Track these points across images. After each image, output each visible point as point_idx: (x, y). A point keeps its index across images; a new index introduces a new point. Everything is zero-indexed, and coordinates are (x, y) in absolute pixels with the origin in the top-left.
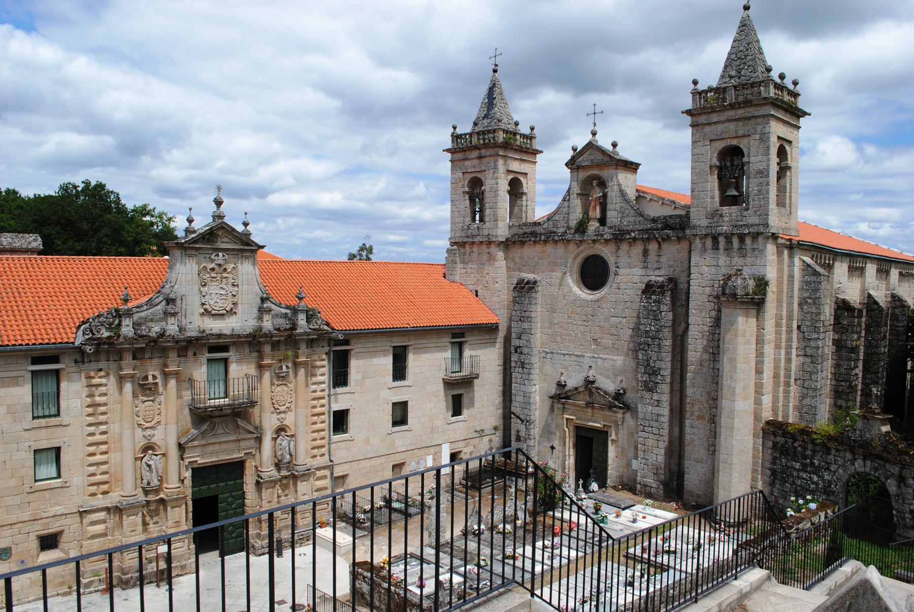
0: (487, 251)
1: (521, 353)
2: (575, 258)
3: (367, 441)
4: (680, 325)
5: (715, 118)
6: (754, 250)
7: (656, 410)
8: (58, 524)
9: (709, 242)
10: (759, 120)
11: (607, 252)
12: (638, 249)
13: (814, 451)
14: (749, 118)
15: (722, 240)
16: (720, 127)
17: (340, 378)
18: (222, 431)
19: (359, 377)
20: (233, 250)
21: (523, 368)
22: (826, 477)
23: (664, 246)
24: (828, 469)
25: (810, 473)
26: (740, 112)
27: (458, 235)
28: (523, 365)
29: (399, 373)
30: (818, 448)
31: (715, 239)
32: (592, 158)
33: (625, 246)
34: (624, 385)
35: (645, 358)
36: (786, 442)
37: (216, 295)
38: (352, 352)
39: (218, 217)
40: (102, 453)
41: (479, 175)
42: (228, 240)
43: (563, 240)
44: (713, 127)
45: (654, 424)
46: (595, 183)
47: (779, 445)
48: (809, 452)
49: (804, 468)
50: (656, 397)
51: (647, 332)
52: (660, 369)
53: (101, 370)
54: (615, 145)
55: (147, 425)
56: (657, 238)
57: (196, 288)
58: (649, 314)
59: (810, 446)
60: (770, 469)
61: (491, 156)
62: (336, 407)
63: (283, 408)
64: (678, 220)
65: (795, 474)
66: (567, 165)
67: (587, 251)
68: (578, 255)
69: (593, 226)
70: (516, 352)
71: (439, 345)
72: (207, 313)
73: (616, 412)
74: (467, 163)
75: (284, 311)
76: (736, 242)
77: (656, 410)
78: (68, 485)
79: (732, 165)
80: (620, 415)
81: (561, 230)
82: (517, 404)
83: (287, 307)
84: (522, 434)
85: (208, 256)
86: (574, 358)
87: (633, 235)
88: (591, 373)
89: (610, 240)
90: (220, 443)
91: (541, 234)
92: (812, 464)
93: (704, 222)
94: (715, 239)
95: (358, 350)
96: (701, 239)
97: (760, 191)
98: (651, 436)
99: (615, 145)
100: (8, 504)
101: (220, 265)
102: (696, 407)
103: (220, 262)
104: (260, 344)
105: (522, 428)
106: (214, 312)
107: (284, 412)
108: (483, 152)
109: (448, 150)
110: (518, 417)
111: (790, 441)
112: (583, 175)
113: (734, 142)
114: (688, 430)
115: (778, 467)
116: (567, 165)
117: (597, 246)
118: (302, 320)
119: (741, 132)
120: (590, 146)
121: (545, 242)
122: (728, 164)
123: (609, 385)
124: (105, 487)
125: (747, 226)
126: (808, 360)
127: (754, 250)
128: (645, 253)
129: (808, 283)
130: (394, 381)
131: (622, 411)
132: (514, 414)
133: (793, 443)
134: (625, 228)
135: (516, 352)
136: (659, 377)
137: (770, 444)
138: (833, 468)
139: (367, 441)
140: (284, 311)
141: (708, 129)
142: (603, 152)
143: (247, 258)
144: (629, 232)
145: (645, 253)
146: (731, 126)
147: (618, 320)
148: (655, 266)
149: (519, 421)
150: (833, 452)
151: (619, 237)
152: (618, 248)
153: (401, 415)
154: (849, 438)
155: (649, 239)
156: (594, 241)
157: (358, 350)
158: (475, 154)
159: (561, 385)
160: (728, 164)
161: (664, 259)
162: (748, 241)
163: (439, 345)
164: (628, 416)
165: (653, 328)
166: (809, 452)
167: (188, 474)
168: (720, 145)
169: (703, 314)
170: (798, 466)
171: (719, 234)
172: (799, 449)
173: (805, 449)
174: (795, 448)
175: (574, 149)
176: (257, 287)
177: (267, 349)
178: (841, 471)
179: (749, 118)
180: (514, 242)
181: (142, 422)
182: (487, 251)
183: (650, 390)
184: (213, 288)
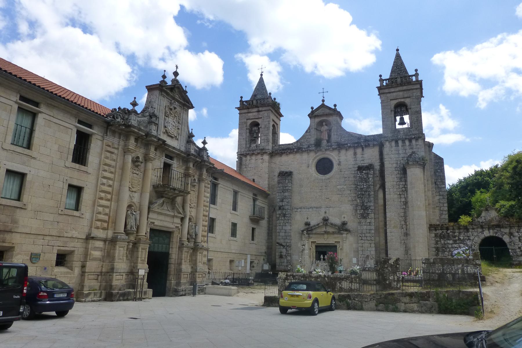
0: (261, 158)
1: (284, 209)
2: (314, 160)
4: (376, 186)
5: (392, 90)
6: (417, 145)
7: (369, 227)
8: (72, 245)
9: (393, 143)
10: (414, 91)
11: (333, 156)
12: (351, 152)
13: (460, 233)
14: (409, 90)
15: (400, 143)
16: (395, 94)
21: (284, 217)
22: (468, 244)
23: (366, 150)
24: (469, 239)
25: (459, 244)
26: (405, 88)
27: (243, 150)
28: (284, 215)
30: (462, 231)
31: (397, 142)
32: (323, 111)
33: (343, 152)
34: (346, 219)
35: (361, 202)
36: (443, 232)
38: (219, 186)
40: (108, 200)
41: (257, 120)
43: (308, 150)
44: (391, 94)
45: (368, 235)
46: (324, 124)
47: (438, 235)
48: (457, 234)
49: (455, 242)
50: (368, 221)
51: (361, 189)
52: (370, 206)
54: (335, 106)
56: (362, 146)
58: (362, 180)
59: (457, 231)
60: (435, 248)
61: (265, 110)
64: (372, 138)
65: (450, 246)
66: (309, 115)
67: (320, 155)
68: (315, 158)
69: (324, 143)
70: (280, 209)
73: (342, 234)
74: (249, 114)
75: (196, 149)
76: (407, 143)
77: (369, 227)
79: (401, 111)
80: (344, 235)
81: (305, 147)
82: (280, 237)
84: (284, 254)
86: (315, 209)
87: (349, 145)
88: (327, 215)
89: (336, 149)
91: (294, 149)
92: (459, 239)
93: (390, 135)
94: (397, 142)
96: (389, 142)
97: (417, 120)
98: (366, 242)
99: (335, 106)
100: (45, 219)
102: (392, 222)
105: (284, 250)
108: (260, 109)
109: (238, 108)
110: (281, 245)
111: (445, 231)
112: (317, 120)
113: (402, 100)
114: (388, 234)
115: (439, 245)
116: (309, 115)
117: (328, 152)
119: (406, 96)
120: (323, 106)
121: (296, 152)
122: (399, 110)
123: (336, 221)
125: (413, 134)
126: (441, 197)
127: (417, 145)
128: (355, 154)
129: (437, 163)
131: (346, 233)
132: (278, 243)
133: (447, 232)
134: (343, 143)
135: (280, 209)
136: (370, 210)
137: (433, 235)
138: (472, 238)
141: (389, 95)
142: (330, 109)
144: (347, 144)
145: (355, 154)
146: (401, 93)
147: (341, 187)
148: (361, 159)
149: (282, 247)
150: (470, 230)
151: (340, 147)
152: (340, 152)
154: (479, 222)
155: (357, 147)
156: (326, 150)
158: (255, 110)
159: (307, 224)
160: (399, 110)
161: (365, 156)
162: (414, 142)
164: (349, 235)
165: (365, 186)
166: (457, 234)
167: (149, 230)
168: (394, 102)
169: (393, 176)
170: (451, 242)
171: (399, 139)
172: (451, 233)
173: (454, 233)
174: (448, 233)
175: (312, 108)
178: (476, 238)
179: (409, 90)
180: (276, 154)
182: (261, 158)
183: (365, 218)
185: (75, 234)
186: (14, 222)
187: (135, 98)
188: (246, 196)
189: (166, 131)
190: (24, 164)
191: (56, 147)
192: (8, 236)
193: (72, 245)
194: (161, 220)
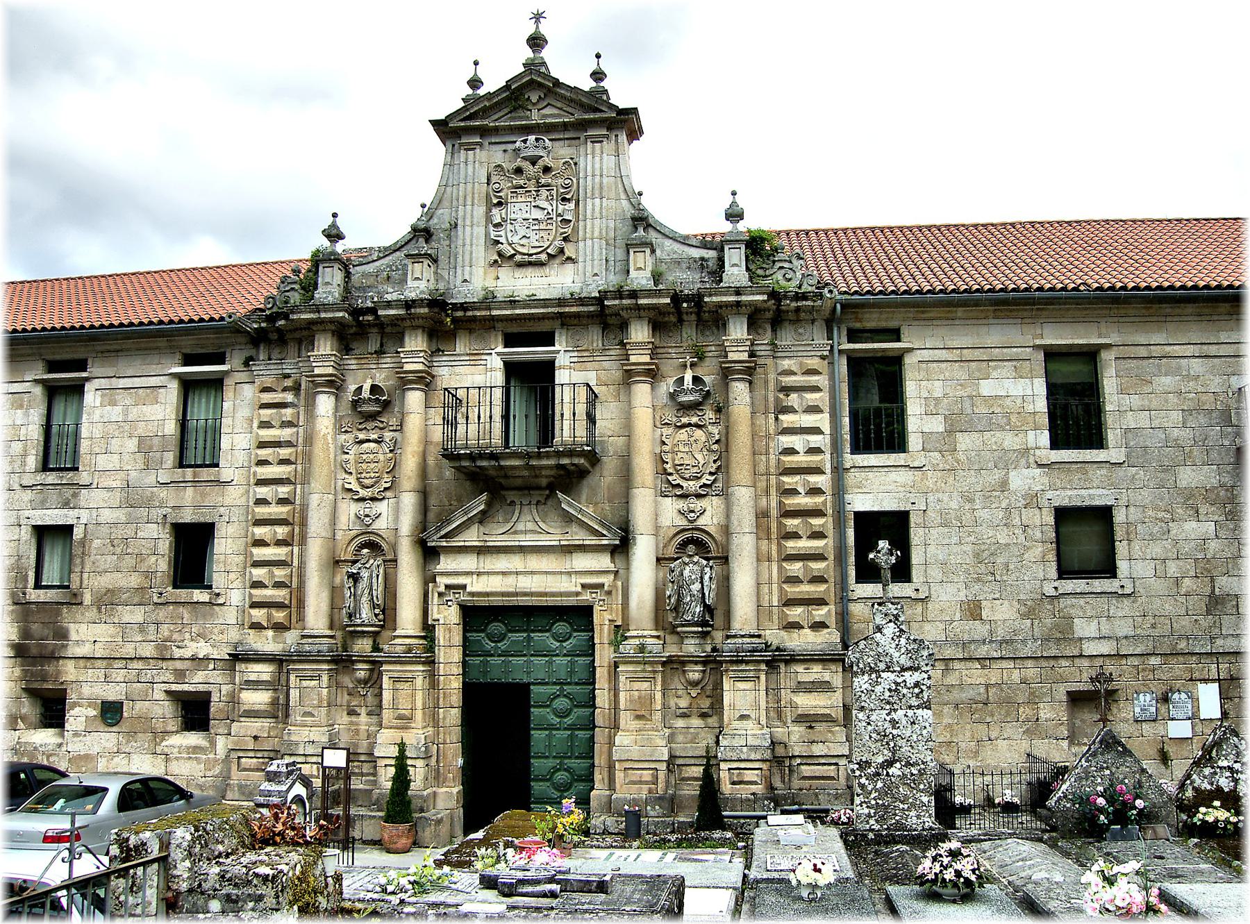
3: (973, 611)
17: (877, 423)
18: (530, 526)
19: (936, 425)
20: (565, 127)
29: (1076, 417)
37: (526, 221)
38: (909, 360)
39: (532, 67)
40: (279, 543)
42: (556, 111)
53: (287, 376)
55: (363, 493)
57: (480, 210)
62: (860, 502)
63: (692, 486)
71: (1213, 350)
72: (503, 259)
75: (697, 253)
78: (221, 601)
83: (705, 245)
85: (510, 147)
90: (522, 550)
95: (926, 355)
100: (125, 620)
101: (534, 161)
103: (530, 153)
104: (624, 326)
106: (518, 258)
107: (699, 496)
118: (736, 271)
124: (279, 616)
130: (1055, 445)
139: (973, 611)
140: (697, 253)
143: (597, 140)
153: (1085, 539)
157: (926, 355)
163: (1213, 350)
176: (625, 203)
177: (640, 333)
181: (354, 486)
184: (520, 209)
185: (202, 649)
186: (63, 635)
187: (335, 215)
188: (1189, 350)
189: (500, 254)
190: (66, 505)
191: (132, 445)
192: (50, 668)
193: (200, 676)
194: (504, 573)
